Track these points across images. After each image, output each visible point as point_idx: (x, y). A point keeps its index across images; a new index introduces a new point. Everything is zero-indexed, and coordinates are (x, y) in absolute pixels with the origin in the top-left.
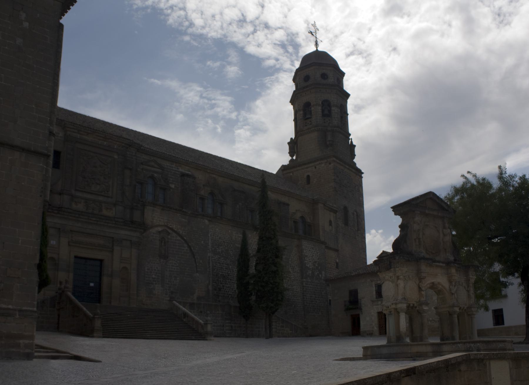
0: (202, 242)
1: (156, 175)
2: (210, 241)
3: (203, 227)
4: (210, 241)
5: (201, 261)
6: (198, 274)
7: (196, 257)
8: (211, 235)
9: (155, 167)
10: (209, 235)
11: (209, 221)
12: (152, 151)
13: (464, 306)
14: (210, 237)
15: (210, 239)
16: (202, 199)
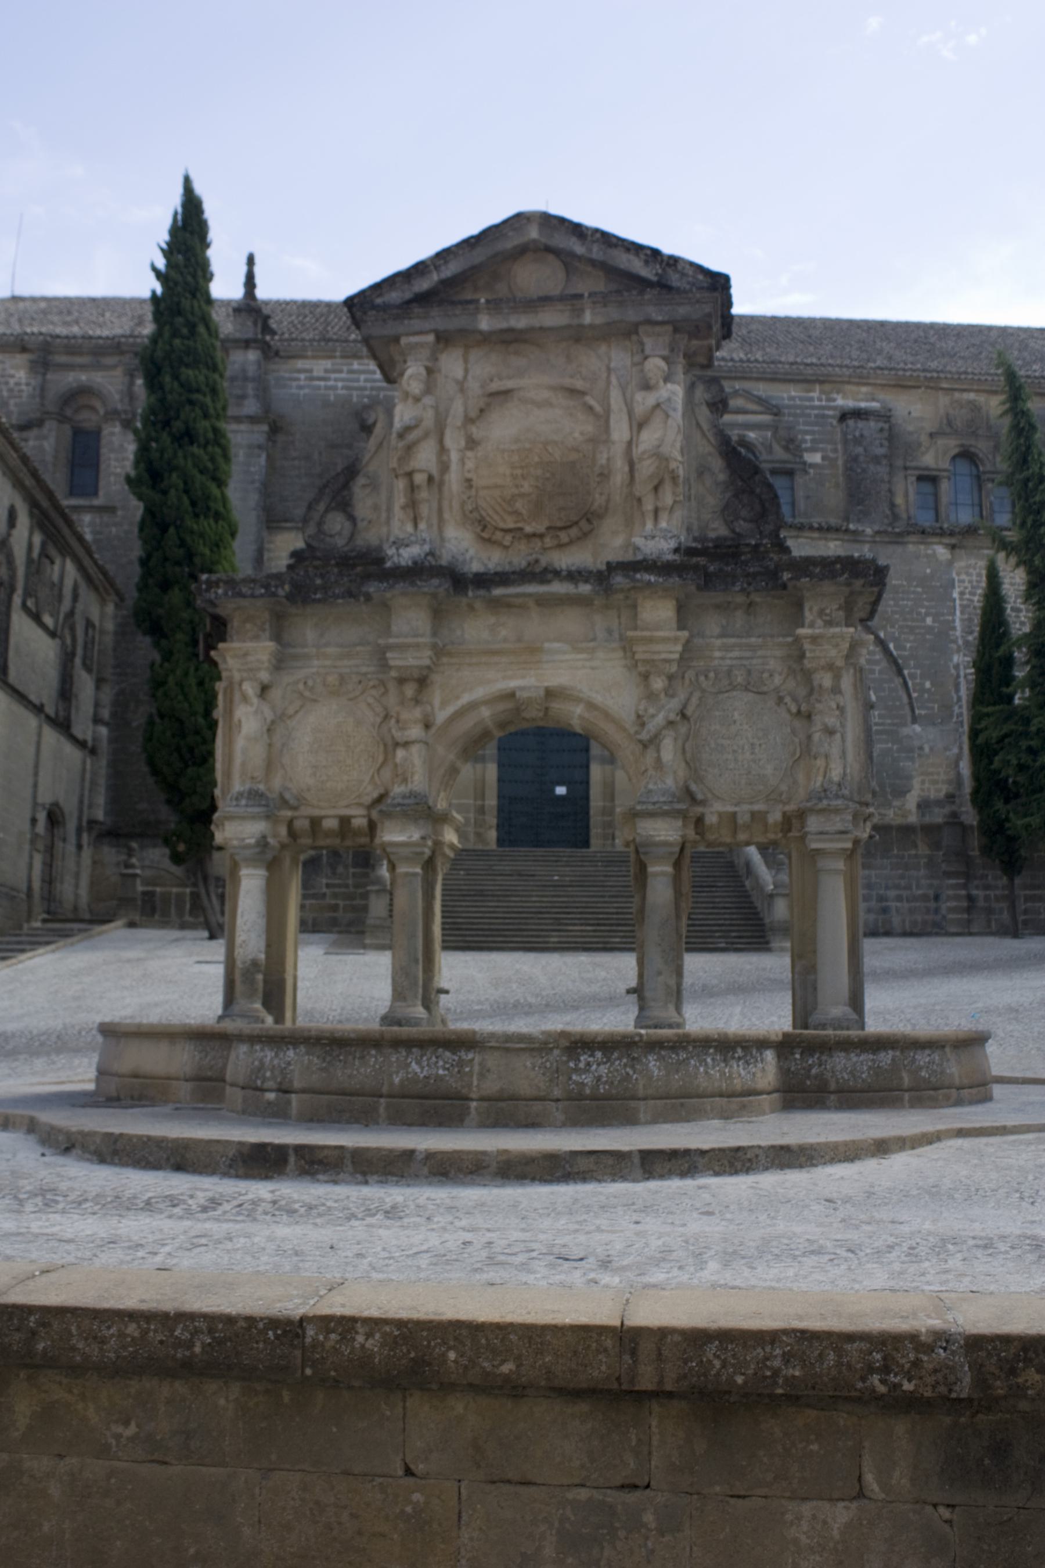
0: (929, 621)
1: (752, 435)
2: (958, 613)
3: (928, 571)
4: (958, 613)
5: (928, 685)
6: (917, 728)
7: (906, 672)
8: (962, 593)
9: (746, 412)
10: (956, 595)
11: (953, 547)
12: (730, 364)
13: (758, 807)
14: (958, 602)
15: (958, 607)
16: (929, 479)
